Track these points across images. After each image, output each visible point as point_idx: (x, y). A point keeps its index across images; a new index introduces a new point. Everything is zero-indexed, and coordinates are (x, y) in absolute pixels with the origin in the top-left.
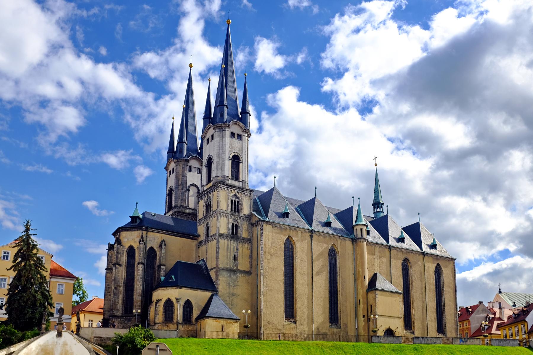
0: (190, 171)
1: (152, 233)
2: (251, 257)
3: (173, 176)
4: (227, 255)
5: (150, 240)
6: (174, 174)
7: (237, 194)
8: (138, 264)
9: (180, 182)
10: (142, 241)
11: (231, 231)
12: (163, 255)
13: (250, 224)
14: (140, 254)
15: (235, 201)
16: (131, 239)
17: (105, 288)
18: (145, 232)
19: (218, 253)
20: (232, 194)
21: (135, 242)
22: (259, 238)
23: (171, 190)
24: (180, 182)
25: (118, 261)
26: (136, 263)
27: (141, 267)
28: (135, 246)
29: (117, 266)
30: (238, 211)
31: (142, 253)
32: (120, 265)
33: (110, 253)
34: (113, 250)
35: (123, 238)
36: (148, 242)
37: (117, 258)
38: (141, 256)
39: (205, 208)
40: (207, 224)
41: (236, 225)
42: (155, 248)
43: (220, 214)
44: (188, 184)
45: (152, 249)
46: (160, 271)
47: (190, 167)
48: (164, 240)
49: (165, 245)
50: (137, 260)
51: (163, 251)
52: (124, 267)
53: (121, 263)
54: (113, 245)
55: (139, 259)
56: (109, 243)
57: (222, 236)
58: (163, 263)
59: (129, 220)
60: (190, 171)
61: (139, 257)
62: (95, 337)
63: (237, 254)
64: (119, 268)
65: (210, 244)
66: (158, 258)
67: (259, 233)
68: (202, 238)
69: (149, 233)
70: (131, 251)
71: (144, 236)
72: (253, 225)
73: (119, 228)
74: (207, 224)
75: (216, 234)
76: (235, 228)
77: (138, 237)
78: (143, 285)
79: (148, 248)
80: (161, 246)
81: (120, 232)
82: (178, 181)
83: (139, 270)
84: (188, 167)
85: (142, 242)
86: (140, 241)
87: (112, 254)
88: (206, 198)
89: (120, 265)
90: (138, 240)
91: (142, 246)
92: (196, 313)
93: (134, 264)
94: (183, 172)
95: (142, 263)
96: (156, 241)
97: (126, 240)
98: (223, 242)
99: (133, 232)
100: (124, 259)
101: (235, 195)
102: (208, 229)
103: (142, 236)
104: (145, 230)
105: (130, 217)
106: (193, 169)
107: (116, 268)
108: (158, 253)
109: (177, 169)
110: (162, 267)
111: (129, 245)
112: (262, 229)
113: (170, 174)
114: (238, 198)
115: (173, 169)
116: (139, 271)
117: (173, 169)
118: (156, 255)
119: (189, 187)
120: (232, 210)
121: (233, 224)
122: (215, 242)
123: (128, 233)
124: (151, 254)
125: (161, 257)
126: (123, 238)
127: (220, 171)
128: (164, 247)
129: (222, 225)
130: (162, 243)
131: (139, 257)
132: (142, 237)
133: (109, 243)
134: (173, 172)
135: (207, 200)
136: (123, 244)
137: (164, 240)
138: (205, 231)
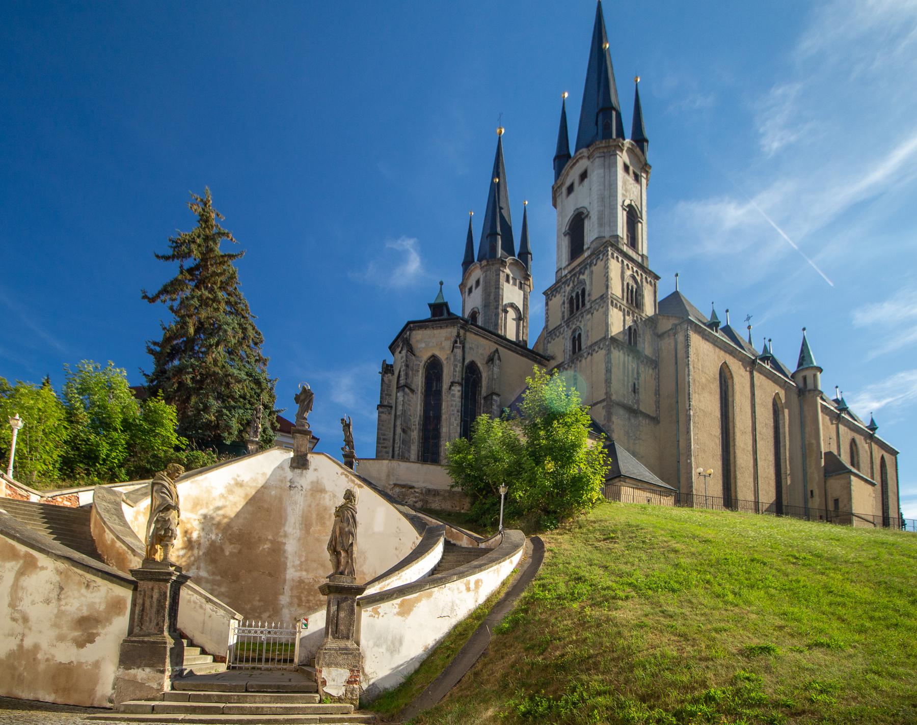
0: (508, 281)
1: (473, 335)
3: (478, 293)
6: (480, 287)
8: (452, 384)
9: (492, 297)
10: (459, 342)
11: (627, 337)
13: (654, 334)
14: (456, 366)
16: (435, 343)
17: (378, 439)
19: (608, 371)
22: (681, 353)
24: (492, 297)
25: (409, 381)
26: (445, 386)
27: (457, 390)
28: (442, 356)
29: (406, 390)
32: (412, 391)
33: (386, 379)
34: (393, 374)
35: (417, 341)
36: (467, 350)
37: (407, 375)
38: (457, 369)
40: (574, 331)
42: (479, 365)
43: (612, 302)
45: (473, 364)
46: (492, 404)
47: (508, 276)
48: (497, 350)
49: (499, 359)
50: (446, 380)
51: (496, 370)
52: (419, 394)
53: (413, 387)
54: (392, 366)
55: (454, 376)
56: (384, 361)
57: (613, 340)
58: (497, 391)
61: (450, 373)
62: (395, 485)
64: (411, 395)
66: (484, 383)
67: (680, 346)
69: (468, 334)
70: (434, 367)
72: (660, 336)
75: (604, 338)
76: (631, 333)
77: (447, 339)
79: (467, 362)
80: (490, 360)
81: (411, 330)
82: (489, 295)
83: (453, 395)
85: (458, 345)
86: (456, 342)
87: (390, 381)
89: (412, 391)
90: (448, 345)
91: (459, 352)
93: (439, 393)
94: (498, 281)
95: (460, 384)
96: (480, 351)
97: (423, 345)
98: (618, 356)
99: (437, 332)
100: (419, 381)
102: (576, 341)
104: (462, 328)
106: (511, 281)
107: (405, 394)
108: (484, 375)
109: (486, 276)
110: (495, 397)
111: (430, 354)
112: (687, 338)
113: (470, 290)
115: (478, 283)
116: (452, 401)
122: (602, 353)
123: (428, 332)
124: (471, 377)
125: (491, 379)
126: (417, 341)
127: (607, 228)
128: (498, 362)
129: (617, 322)
132: (458, 336)
133: (384, 361)
137: (497, 350)
138: (569, 345)
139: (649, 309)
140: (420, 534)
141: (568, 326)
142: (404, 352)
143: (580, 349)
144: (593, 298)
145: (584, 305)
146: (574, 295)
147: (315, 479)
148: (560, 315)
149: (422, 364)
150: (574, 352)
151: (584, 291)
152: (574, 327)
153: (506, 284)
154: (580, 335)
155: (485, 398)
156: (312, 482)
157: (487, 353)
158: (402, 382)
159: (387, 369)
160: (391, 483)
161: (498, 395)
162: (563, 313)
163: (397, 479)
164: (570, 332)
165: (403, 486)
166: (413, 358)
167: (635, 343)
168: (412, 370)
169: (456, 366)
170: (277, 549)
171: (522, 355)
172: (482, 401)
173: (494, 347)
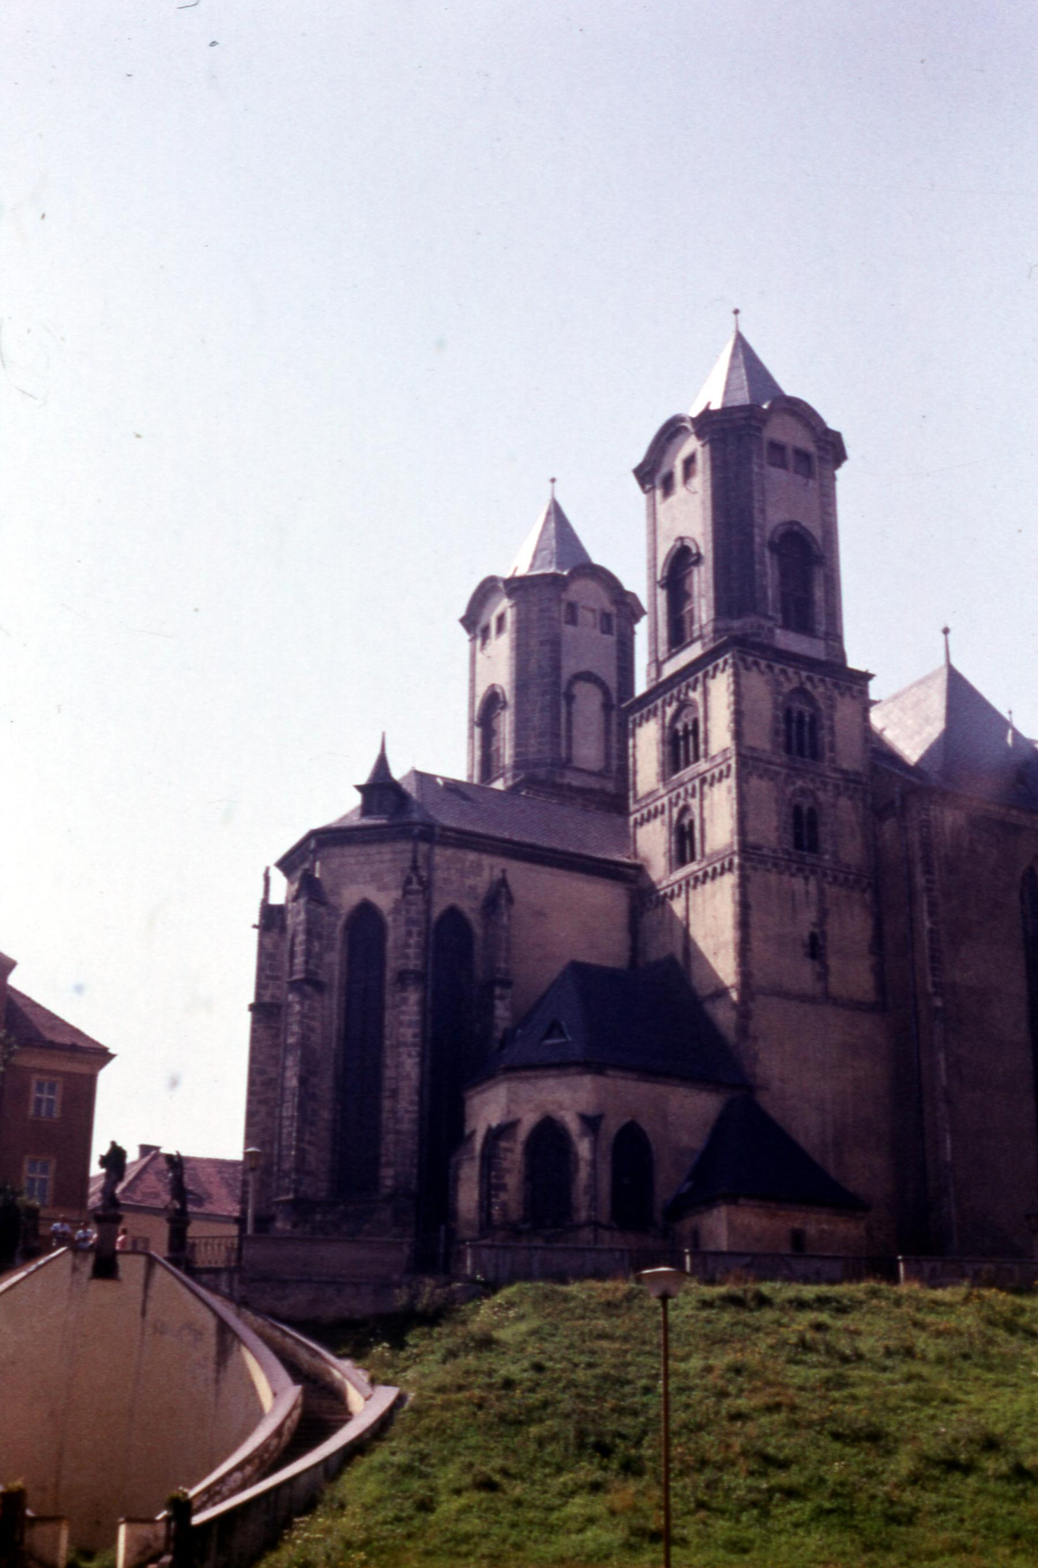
0: (573, 620)
2: (878, 942)
3: (501, 648)
7: (809, 686)
15: (801, 714)
18: (423, 847)
20: (787, 688)
21: (382, 888)
23: (492, 702)
26: (389, 975)
28: (384, 901)
29: (308, 989)
30: (816, 754)
31: (415, 929)
37: (308, 954)
41: (811, 811)
44: (566, 675)
47: (572, 607)
48: (503, 882)
49: (510, 900)
50: (393, 963)
53: (323, 977)
59: (356, 799)
60: (573, 620)
63: (824, 934)
68: (659, 870)
71: (421, 861)
73: (313, 834)
74: (685, 810)
78: (422, 1064)
79: (437, 912)
84: (563, 607)
86: (409, 881)
88: (670, 711)
92: (668, 1181)
101: (800, 691)
103: (415, 860)
105: (360, 788)
114: (810, 700)
115: (501, 619)
117: (501, 619)
119: (571, 683)
120: (788, 749)
121: (797, 810)
130: (498, 897)
131: (402, 947)
132: (415, 868)
134: (500, 628)
135: (676, 717)
136: (332, 900)
142: (302, 901)
146: (679, 726)
149: (341, 923)
151: (696, 722)
153: (569, 630)
154: (692, 823)
159: (271, 919)
167: (814, 847)
168: (320, 937)
169: (409, 934)
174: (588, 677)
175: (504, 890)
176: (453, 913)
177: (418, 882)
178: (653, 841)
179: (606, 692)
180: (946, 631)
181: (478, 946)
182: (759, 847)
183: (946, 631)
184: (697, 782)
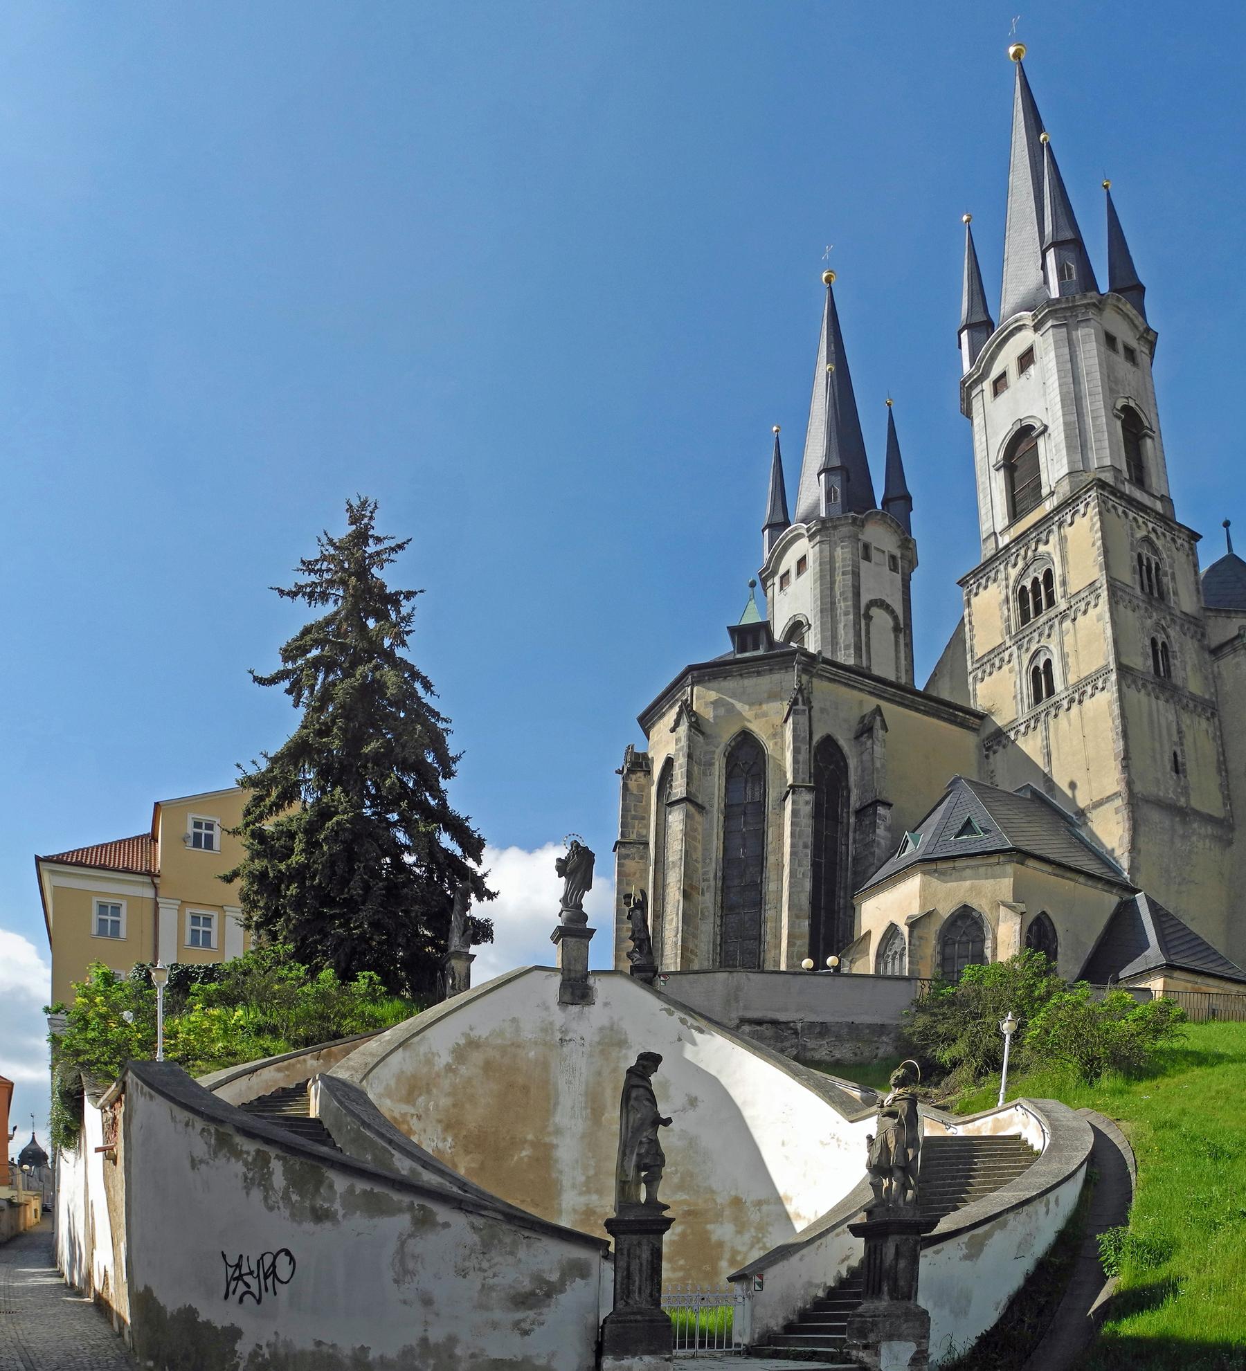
4: (1154, 750)
5: (822, 710)
12: (878, 764)
25: (693, 790)
29: (692, 809)
39: (1014, 605)
40: (1036, 654)
42: (842, 742)
45: (829, 741)
48: (878, 710)
56: (630, 748)
58: (885, 796)
64: (698, 818)
65: (1066, 726)
69: (814, 680)
70: (746, 757)
75: (1105, 671)
80: (865, 729)
89: (701, 808)
95: (809, 789)
111: (735, 729)
118: (846, 766)
128: (881, 732)
137: (878, 710)
138: (1027, 687)
139: (1186, 601)
140: (851, 1111)
141: (1019, 648)
143: (1051, 692)
144: (1072, 590)
145: (1051, 602)
147: (606, 1023)
148: (1000, 625)
150: (1038, 699)
152: (1034, 647)
154: (1048, 663)
155: (858, 812)
156: (601, 1029)
157: (855, 715)
158: (679, 788)
160: (734, 1015)
161: (888, 805)
162: (1008, 619)
163: (746, 1008)
164: (1026, 658)
165: (759, 1022)
166: (701, 738)
168: (699, 764)
169: (796, 751)
170: (544, 1157)
171: (926, 713)
172: (852, 820)
173: (872, 702)
174: (880, 604)
175: (878, 718)
176: (829, 741)
177: (801, 703)
178: (999, 693)
179: (895, 618)
180: (1227, 524)
181: (853, 778)
182: (1132, 669)
183: (1227, 524)
184: (1056, 621)
